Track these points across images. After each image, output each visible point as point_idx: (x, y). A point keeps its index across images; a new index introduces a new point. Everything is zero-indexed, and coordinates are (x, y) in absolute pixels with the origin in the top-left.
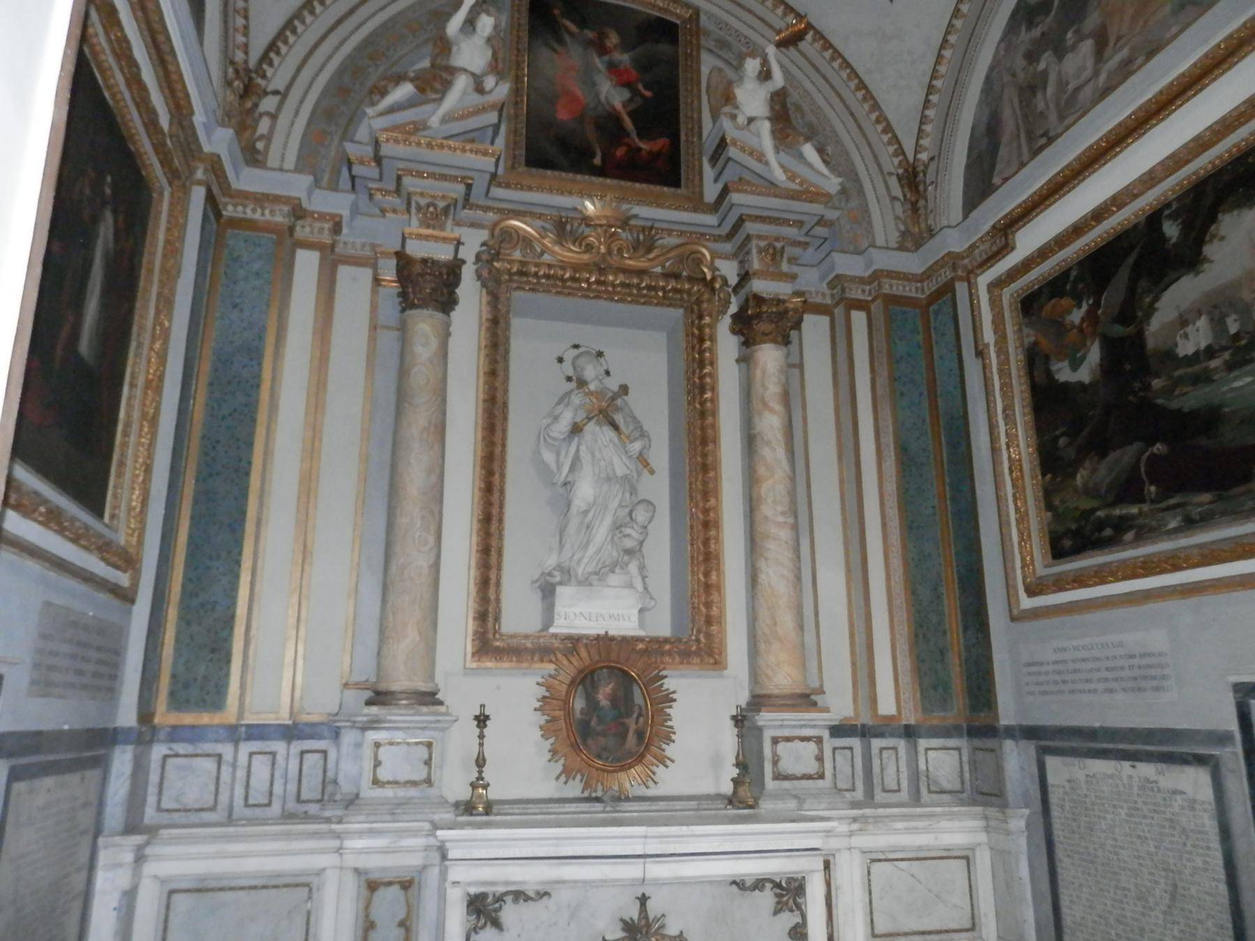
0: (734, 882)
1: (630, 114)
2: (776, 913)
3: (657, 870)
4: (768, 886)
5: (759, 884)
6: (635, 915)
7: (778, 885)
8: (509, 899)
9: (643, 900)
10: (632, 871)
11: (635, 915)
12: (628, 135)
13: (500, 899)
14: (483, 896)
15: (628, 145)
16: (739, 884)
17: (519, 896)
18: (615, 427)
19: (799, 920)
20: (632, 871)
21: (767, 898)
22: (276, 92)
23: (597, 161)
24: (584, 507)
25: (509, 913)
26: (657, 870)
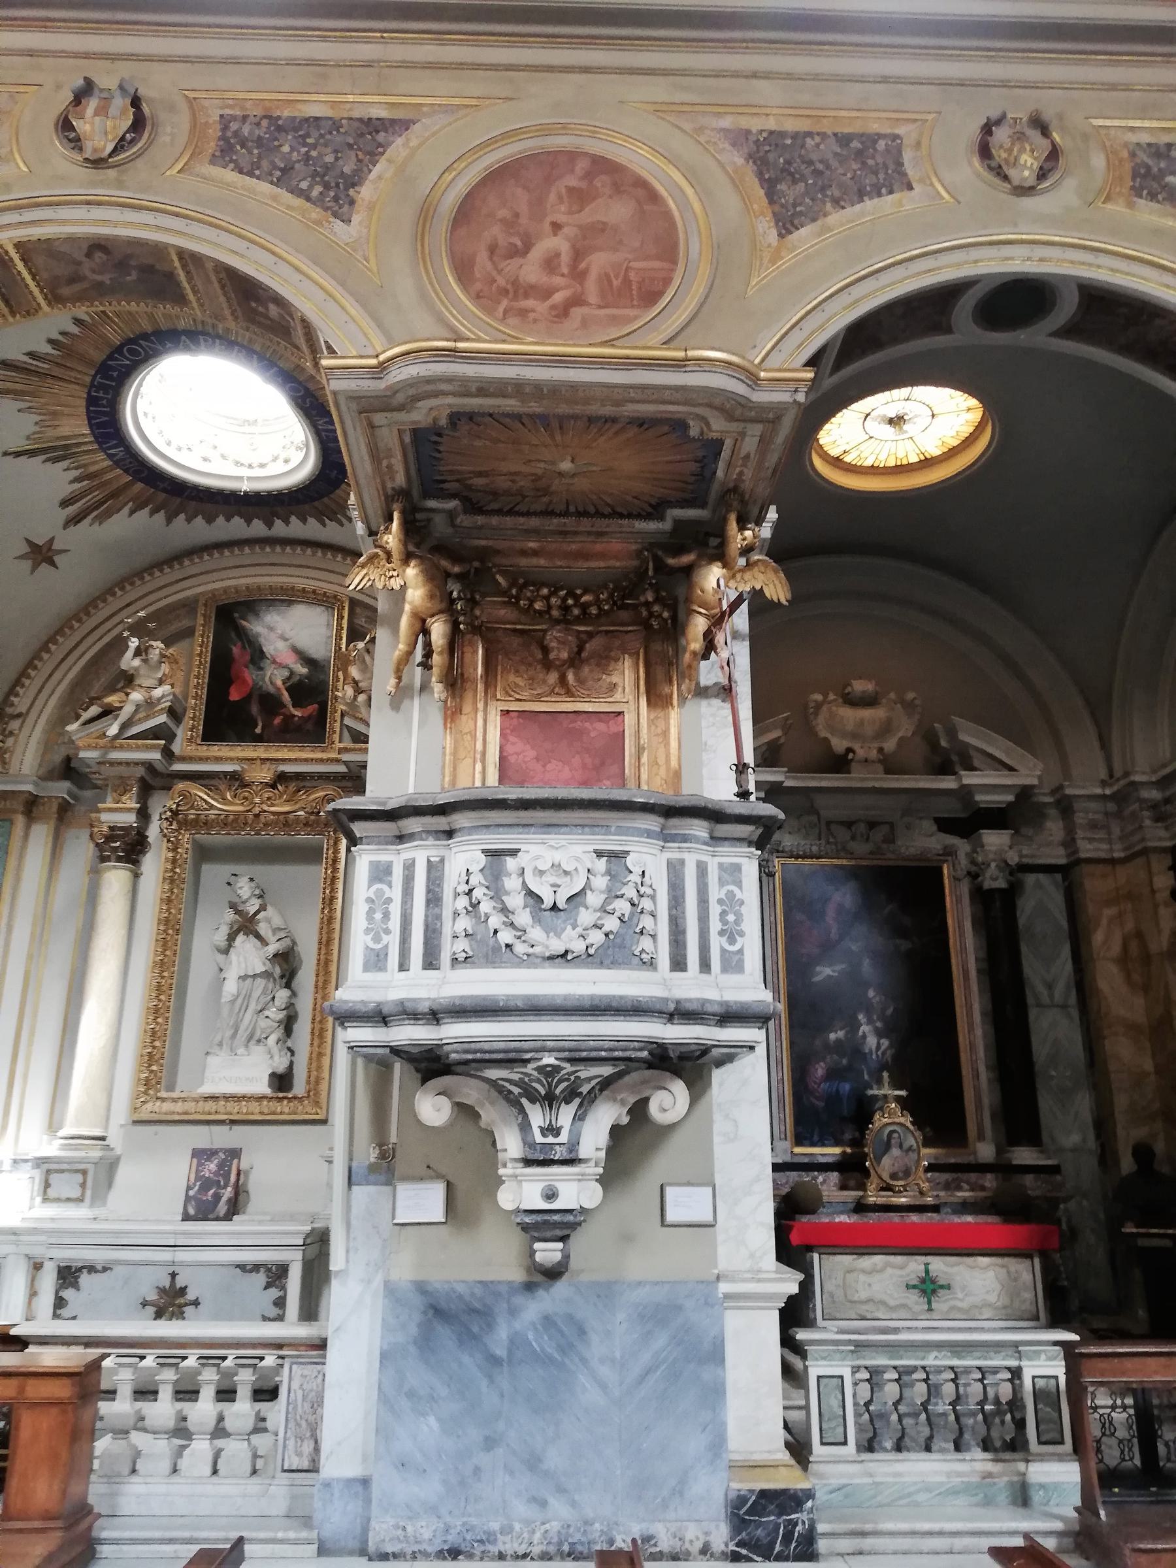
0: (237, 1266)
1: (287, 689)
2: (265, 1289)
3: (182, 1256)
4: (262, 1270)
5: (256, 1268)
6: (167, 1287)
7: (269, 1270)
8: (85, 1271)
9: (173, 1275)
10: (165, 1256)
11: (167, 1287)
12: (284, 706)
13: (80, 1269)
14: (69, 1267)
15: (283, 714)
16: (242, 1267)
17: (91, 1269)
18: (258, 936)
19: (281, 1293)
20: (165, 1256)
21: (261, 1278)
22: (19, 715)
23: (258, 730)
24: (230, 998)
25: (85, 1279)
26: (182, 1256)
